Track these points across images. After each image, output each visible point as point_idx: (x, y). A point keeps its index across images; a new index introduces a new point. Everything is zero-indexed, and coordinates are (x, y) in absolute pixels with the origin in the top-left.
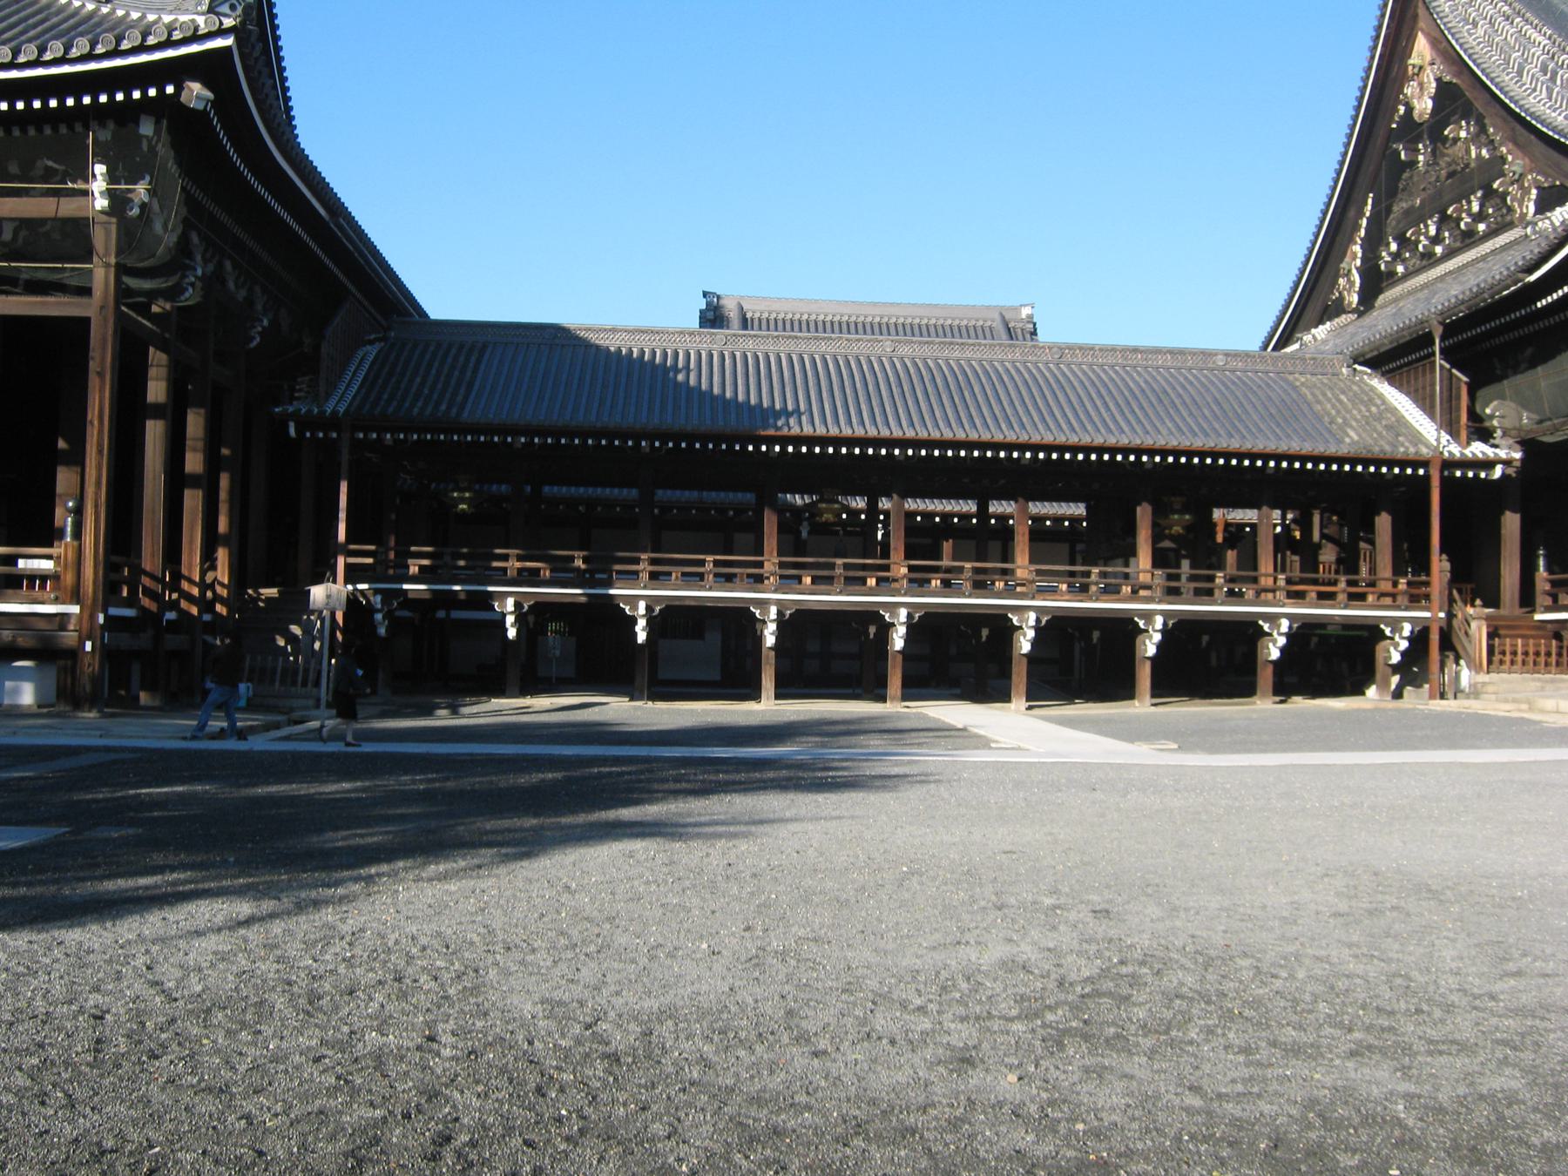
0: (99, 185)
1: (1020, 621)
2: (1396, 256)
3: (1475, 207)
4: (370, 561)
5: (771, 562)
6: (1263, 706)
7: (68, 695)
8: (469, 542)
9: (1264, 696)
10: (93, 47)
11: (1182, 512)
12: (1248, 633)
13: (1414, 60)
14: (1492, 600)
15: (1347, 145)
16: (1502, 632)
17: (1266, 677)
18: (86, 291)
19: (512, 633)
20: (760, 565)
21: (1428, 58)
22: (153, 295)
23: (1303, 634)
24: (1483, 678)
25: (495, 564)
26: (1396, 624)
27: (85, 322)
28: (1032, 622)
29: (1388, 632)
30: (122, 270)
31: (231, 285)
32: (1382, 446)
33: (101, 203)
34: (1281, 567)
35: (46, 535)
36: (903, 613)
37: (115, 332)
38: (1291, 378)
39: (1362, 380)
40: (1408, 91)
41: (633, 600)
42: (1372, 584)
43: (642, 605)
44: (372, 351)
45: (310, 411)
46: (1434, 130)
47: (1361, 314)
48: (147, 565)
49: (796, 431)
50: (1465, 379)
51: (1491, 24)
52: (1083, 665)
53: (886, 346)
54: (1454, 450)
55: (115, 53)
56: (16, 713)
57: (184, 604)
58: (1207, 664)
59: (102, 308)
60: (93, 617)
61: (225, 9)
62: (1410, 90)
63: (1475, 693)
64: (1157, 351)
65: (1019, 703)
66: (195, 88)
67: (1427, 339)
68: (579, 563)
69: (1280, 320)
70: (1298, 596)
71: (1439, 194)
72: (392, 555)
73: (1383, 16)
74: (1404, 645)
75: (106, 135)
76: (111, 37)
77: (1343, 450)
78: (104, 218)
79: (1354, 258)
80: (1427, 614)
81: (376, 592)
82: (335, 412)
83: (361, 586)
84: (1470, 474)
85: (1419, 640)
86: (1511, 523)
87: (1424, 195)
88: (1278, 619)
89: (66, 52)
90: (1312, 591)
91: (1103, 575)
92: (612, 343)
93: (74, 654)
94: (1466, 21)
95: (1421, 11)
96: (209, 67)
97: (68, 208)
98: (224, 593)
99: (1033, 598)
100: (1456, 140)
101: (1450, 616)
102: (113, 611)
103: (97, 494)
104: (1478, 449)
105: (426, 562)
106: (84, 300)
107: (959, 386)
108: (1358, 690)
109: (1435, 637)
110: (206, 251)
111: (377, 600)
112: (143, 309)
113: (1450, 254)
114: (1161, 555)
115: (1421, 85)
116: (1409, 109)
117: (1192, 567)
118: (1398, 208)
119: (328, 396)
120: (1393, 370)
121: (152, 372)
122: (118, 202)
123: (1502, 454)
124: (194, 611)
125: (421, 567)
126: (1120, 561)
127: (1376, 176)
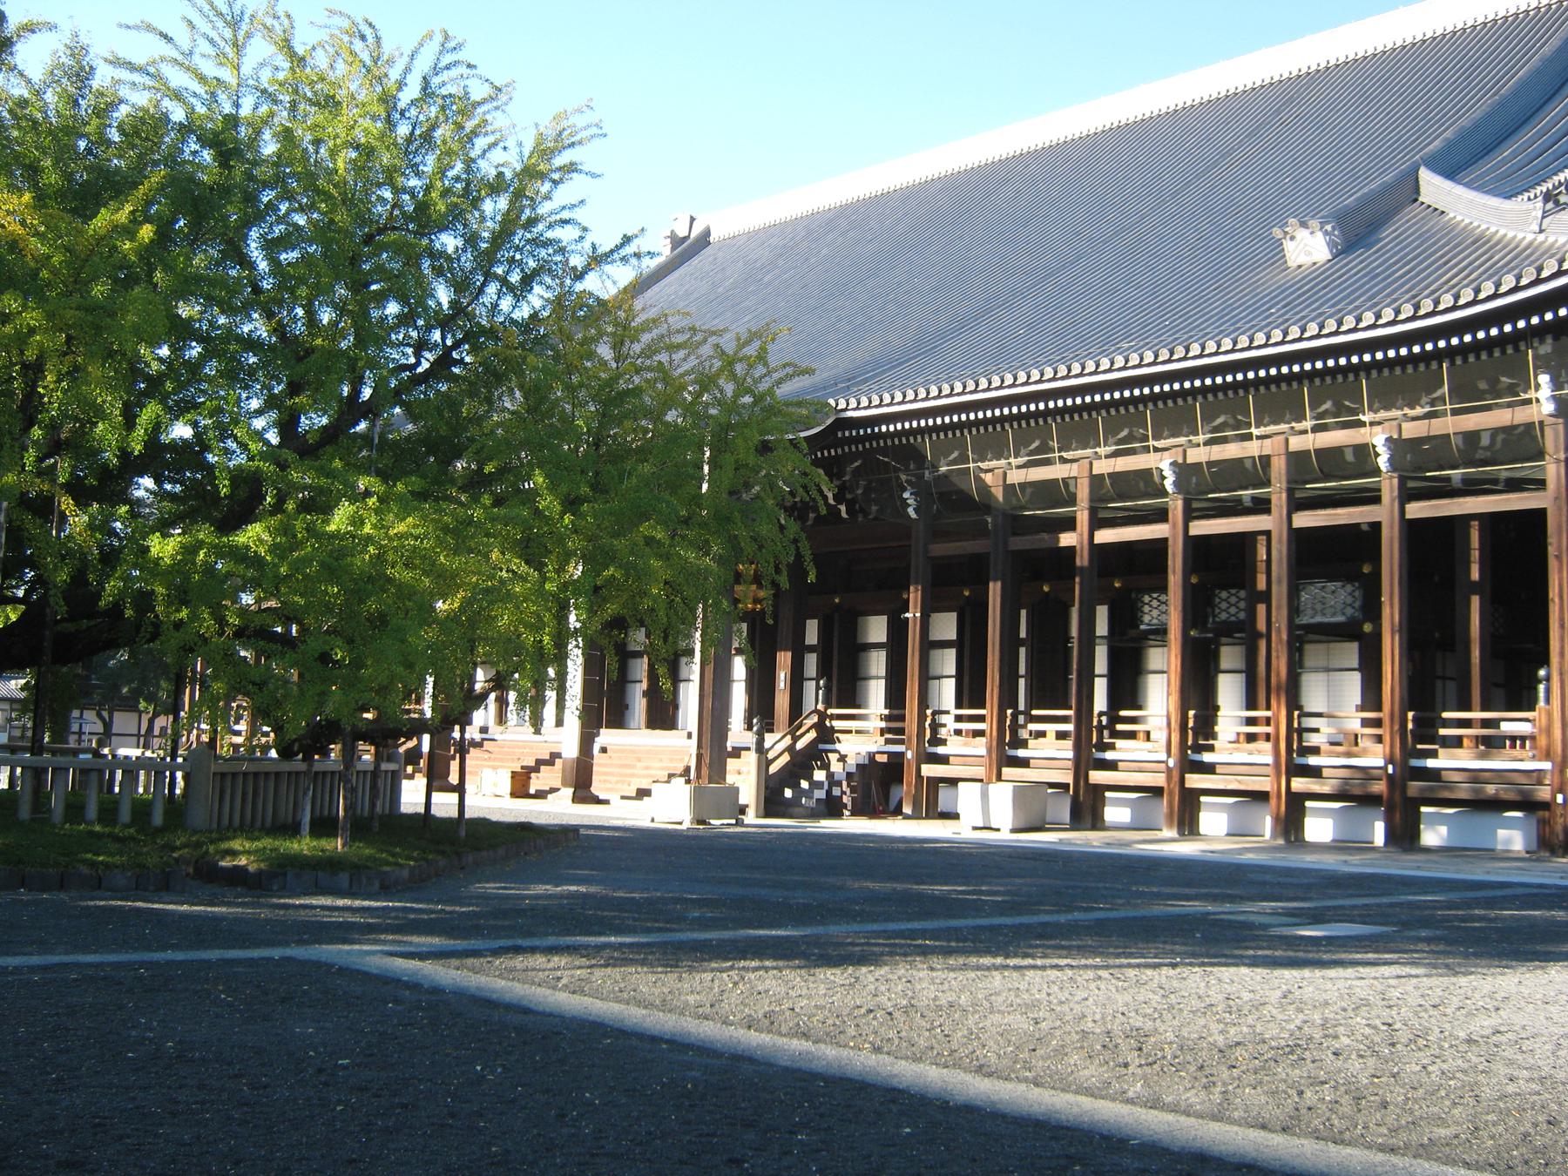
18: (1541, 484)
27: (1542, 513)
33: (1548, 407)
56: (1506, 856)
59: (1556, 498)
75: (1546, 348)
76: (1532, 270)
93: (1546, 806)
97: (1521, 416)
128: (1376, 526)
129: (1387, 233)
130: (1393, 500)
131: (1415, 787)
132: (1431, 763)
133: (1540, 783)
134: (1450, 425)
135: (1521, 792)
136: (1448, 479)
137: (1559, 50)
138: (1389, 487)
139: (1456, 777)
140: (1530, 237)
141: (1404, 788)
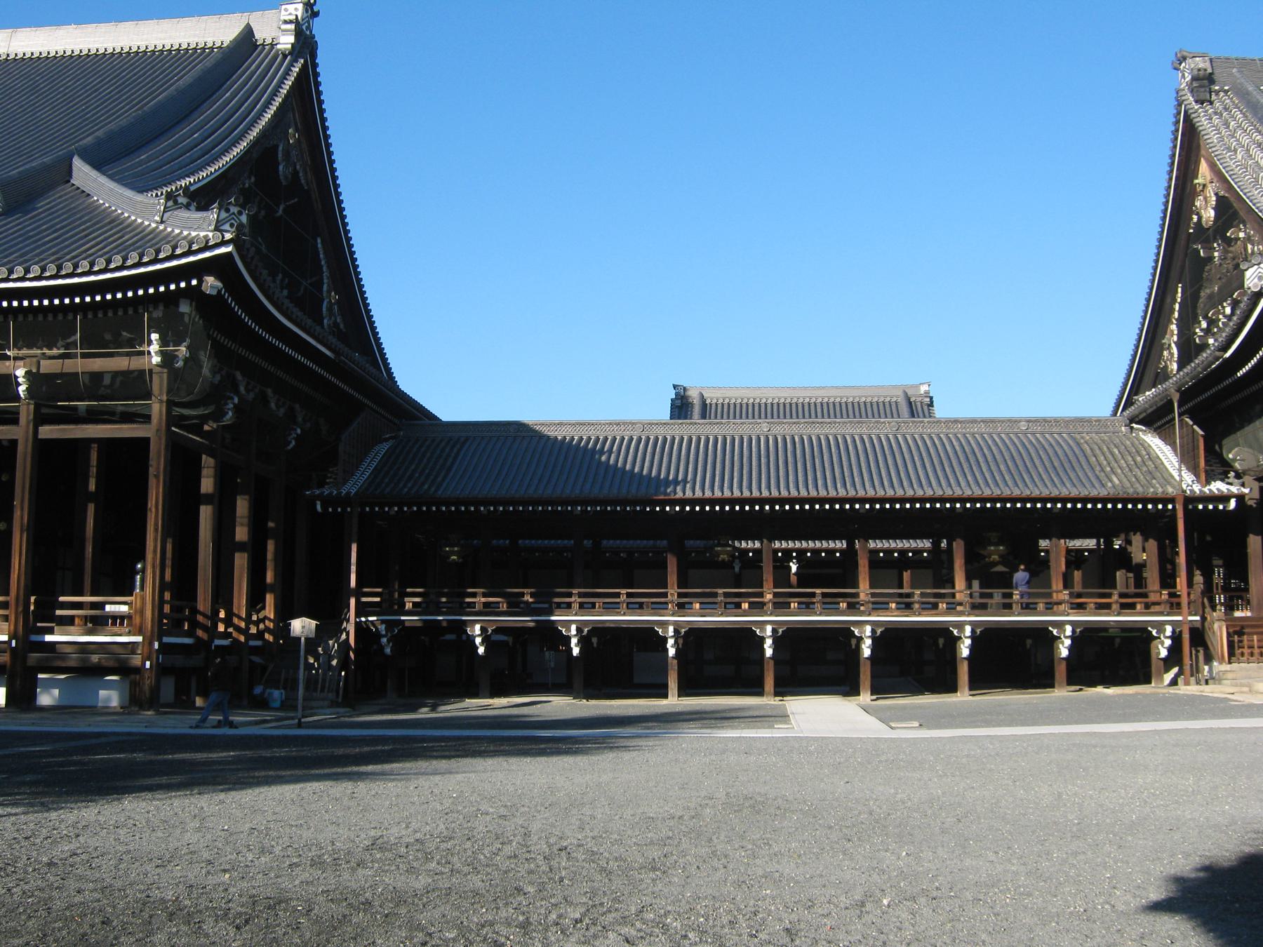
0: (154, 348)
1: (860, 632)
2: (1208, 332)
4: (378, 599)
5: (673, 592)
6: (1061, 693)
7: (135, 701)
8: (452, 585)
9: (1060, 686)
10: (141, 258)
11: (997, 544)
12: (1044, 637)
15: (1159, 247)
16: (1246, 630)
17: (1061, 671)
19: (576, 651)
20: (665, 595)
21: (1209, 178)
22: (204, 419)
23: (1086, 638)
24: (1228, 667)
25: (468, 600)
26: (1160, 626)
27: (146, 441)
28: (868, 633)
29: (1154, 633)
30: (170, 404)
31: (273, 405)
33: (156, 359)
34: (1067, 583)
35: (123, 587)
36: (769, 628)
37: (167, 446)
38: (1078, 436)
39: (1138, 438)
40: (1198, 204)
41: (567, 624)
42: (1145, 595)
43: (574, 627)
44: (384, 448)
45: (331, 493)
48: (201, 607)
49: (680, 495)
50: (1201, 433)
51: (1248, 150)
52: (913, 665)
53: (763, 427)
55: (139, 264)
56: (106, 712)
57: (235, 634)
58: (1013, 662)
60: (151, 644)
61: (227, 227)
64: (974, 421)
65: (866, 697)
66: (210, 280)
67: (1170, 402)
68: (528, 598)
69: (1125, 385)
70: (1080, 607)
72: (396, 595)
73: (1175, 147)
74: (1168, 642)
75: (158, 313)
76: (152, 251)
77: (1103, 493)
78: (159, 369)
79: (1172, 335)
80: (1180, 618)
81: (383, 622)
82: (348, 493)
83: (370, 619)
84: (1211, 507)
85: (1176, 638)
87: (1220, 283)
88: (1065, 624)
89: (124, 262)
90: (1092, 602)
91: (922, 595)
92: (559, 434)
93: (138, 670)
94: (1229, 149)
96: (218, 266)
97: (136, 363)
98: (271, 625)
99: (869, 615)
100: (1238, 239)
101: (1204, 619)
102: (166, 640)
103: (154, 559)
104: (1218, 487)
105: (417, 600)
106: (147, 426)
107: (808, 455)
109: (1186, 636)
110: (248, 384)
111: (382, 628)
112: (197, 430)
114: (965, 578)
115: (1205, 198)
116: (1200, 218)
117: (981, 587)
119: (345, 482)
120: (1159, 427)
121: (205, 472)
122: (168, 358)
124: (242, 639)
125: (414, 603)
127: (1181, 273)
128: (14, 443)
129: (42, 204)
130: (28, 423)
131: (34, 657)
132: (48, 638)
133: (134, 653)
134: (78, 365)
135: (119, 660)
136: (75, 408)
137: (191, 85)
138: (26, 412)
139: (68, 649)
140: (154, 225)
141: (25, 659)
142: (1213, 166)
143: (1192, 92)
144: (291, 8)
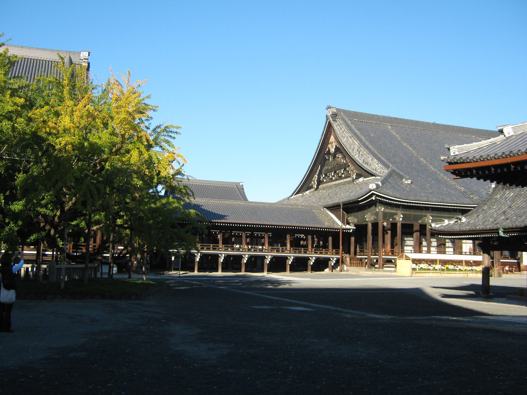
2: (324, 178)
3: (342, 172)
6: (309, 273)
13: (331, 141)
14: (350, 254)
17: (309, 268)
24: (349, 268)
32: (332, 226)
46: (334, 156)
47: (316, 189)
54: (344, 227)
62: (330, 146)
63: (347, 270)
67: (340, 206)
69: (297, 188)
71: (334, 167)
74: (334, 262)
77: (326, 227)
85: (337, 262)
86: (353, 239)
88: (313, 257)
90: (319, 252)
95: (332, 131)
100: (338, 157)
104: (348, 226)
108: (323, 270)
109: (341, 261)
113: (336, 180)
116: (329, 150)
118: (325, 168)
123: (352, 227)
126: (275, 245)
142: (336, 138)
143: (332, 117)
144: (84, 53)
